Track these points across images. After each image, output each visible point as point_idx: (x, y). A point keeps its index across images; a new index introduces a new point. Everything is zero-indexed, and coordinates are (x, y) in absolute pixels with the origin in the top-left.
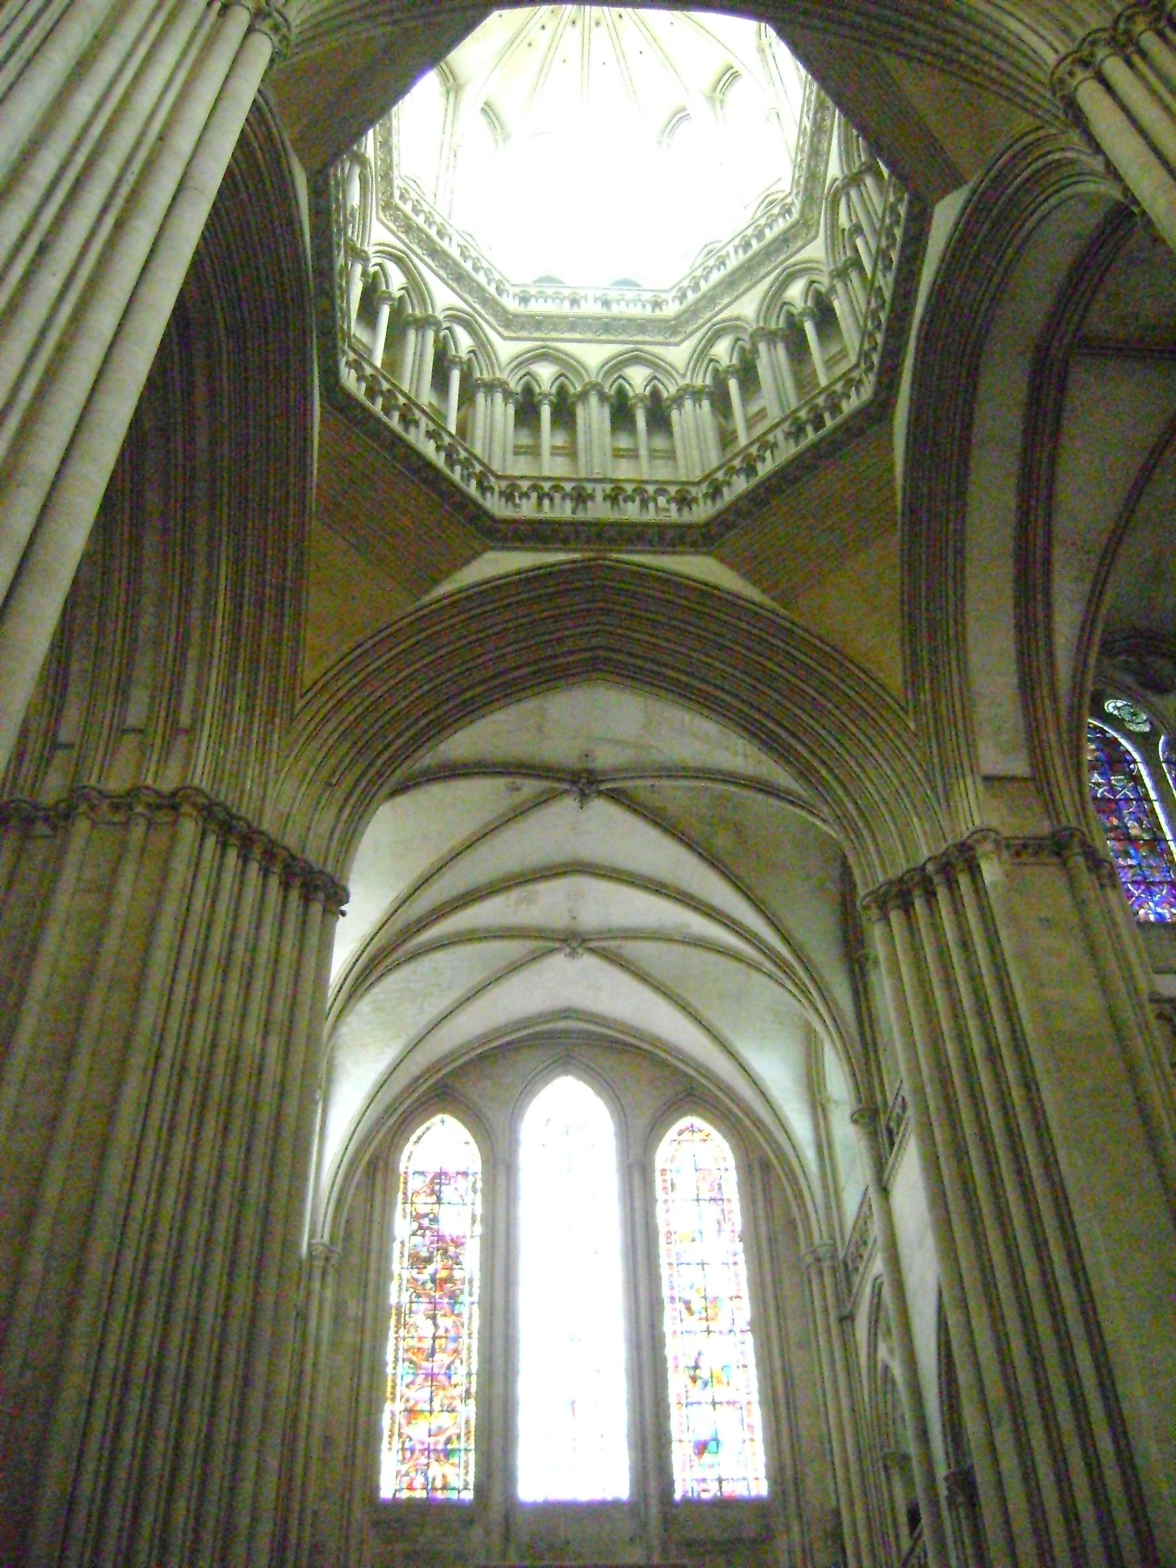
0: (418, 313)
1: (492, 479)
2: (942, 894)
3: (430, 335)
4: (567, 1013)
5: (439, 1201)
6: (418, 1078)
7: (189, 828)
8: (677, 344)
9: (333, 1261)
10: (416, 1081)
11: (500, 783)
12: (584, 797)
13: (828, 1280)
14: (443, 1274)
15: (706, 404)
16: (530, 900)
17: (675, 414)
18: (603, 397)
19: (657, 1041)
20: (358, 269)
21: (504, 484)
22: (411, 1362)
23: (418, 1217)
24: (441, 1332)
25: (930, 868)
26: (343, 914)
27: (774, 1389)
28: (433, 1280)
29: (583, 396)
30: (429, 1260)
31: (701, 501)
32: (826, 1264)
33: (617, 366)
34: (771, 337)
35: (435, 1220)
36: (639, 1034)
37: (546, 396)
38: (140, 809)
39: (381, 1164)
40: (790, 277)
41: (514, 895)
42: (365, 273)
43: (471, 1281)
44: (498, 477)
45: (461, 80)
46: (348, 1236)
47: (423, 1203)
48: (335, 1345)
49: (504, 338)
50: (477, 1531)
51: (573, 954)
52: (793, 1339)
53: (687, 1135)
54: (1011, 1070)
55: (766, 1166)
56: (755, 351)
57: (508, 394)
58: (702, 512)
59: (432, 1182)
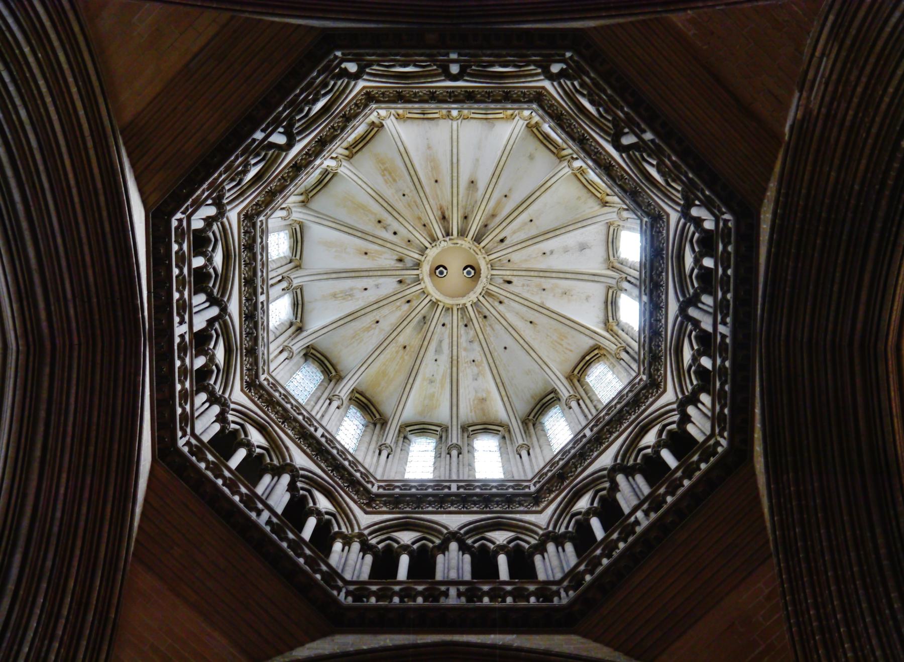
0: (276, 462)
1: (340, 583)
3: (286, 479)
8: (540, 512)
15: (569, 547)
17: (538, 558)
18: (464, 548)
20: (216, 409)
21: (351, 588)
29: (443, 548)
31: (563, 594)
33: (478, 529)
34: (629, 472)
37: (405, 548)
40: (644, 430)
42: (221, 418)
44: (347, 583)
45: (342, 374)
49: (366, 513)
56: (615, 487)
57: (366, 548)
58: (564, 599)
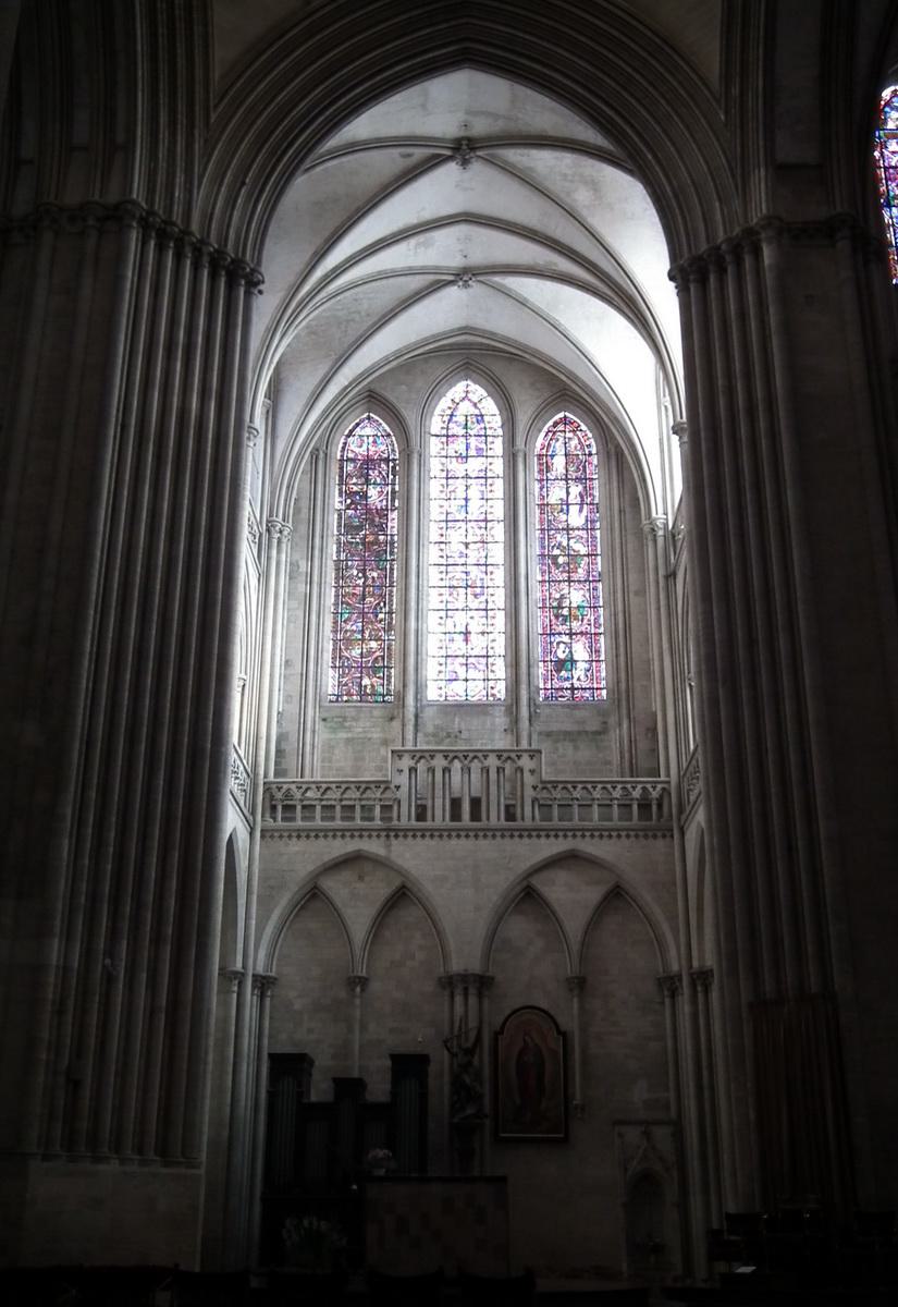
2: (730, 269)
4: (466, 330)
5: (367, 482)
6: (346, 387)
7: (134, 236)
9: (285, 533)
10: (344, 391)
11: (396, 152)
12: (465, 163)
13: (660, 541)
14: (371, 538)
16: (426, 245)
19: (536, 353)
22: (348, 604)
23: (351, 494)
24: (370, 582)
25: (724, 247)
26: (260, 292)
27: (616, 625)
28: (363, 544)
30: (360, 528)
32: (661, 533)
35: (365, 496)
36: (525, 348)
38: (91, 222)
39: (322, 455)
41: (413, 241)
43: (392, 543)
46: (297, 511)
47: (355, 485)
48: (291, 594)
50: (396, 724)
51: (466, 285)
52: (632, 588)
53: (561, 427)
54: (762, 424)
55: (620, 455)
59: (361, 468)
